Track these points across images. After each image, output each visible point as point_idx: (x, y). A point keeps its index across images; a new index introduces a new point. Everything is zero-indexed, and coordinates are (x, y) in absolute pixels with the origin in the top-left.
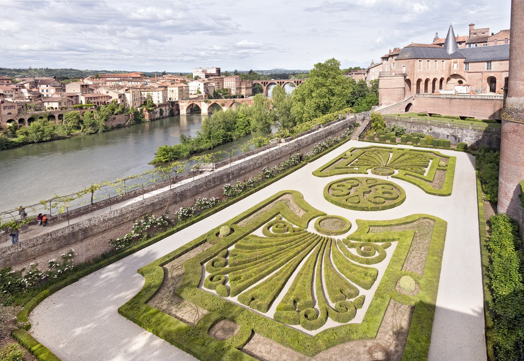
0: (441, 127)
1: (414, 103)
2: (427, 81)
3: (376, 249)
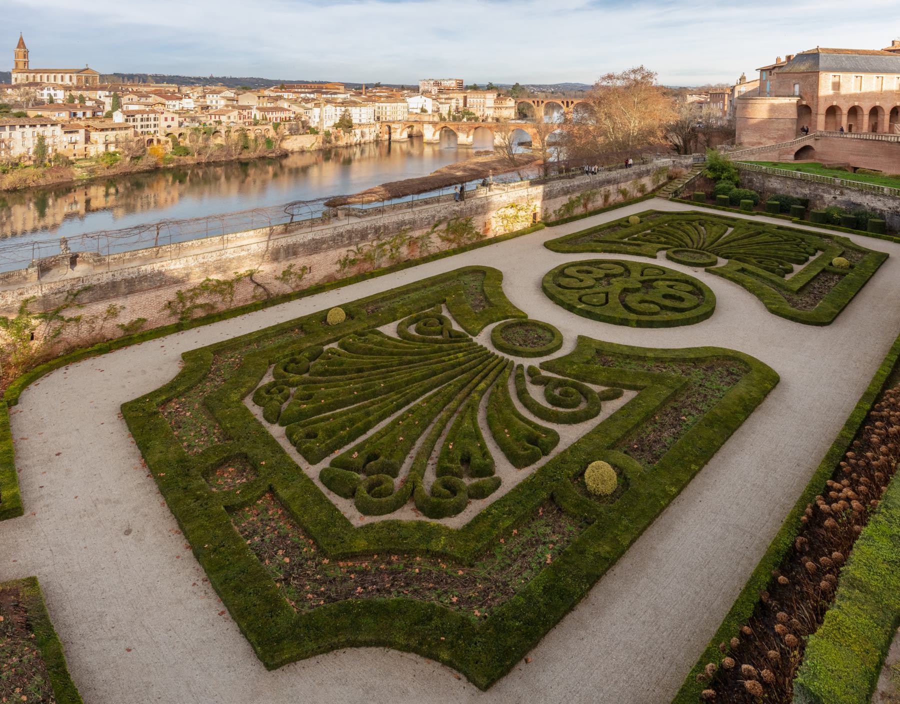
3: (586, 394)
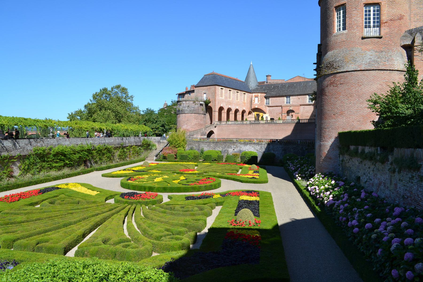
0: (247, 144)
1: (215, 130)
2: (229, 110)
